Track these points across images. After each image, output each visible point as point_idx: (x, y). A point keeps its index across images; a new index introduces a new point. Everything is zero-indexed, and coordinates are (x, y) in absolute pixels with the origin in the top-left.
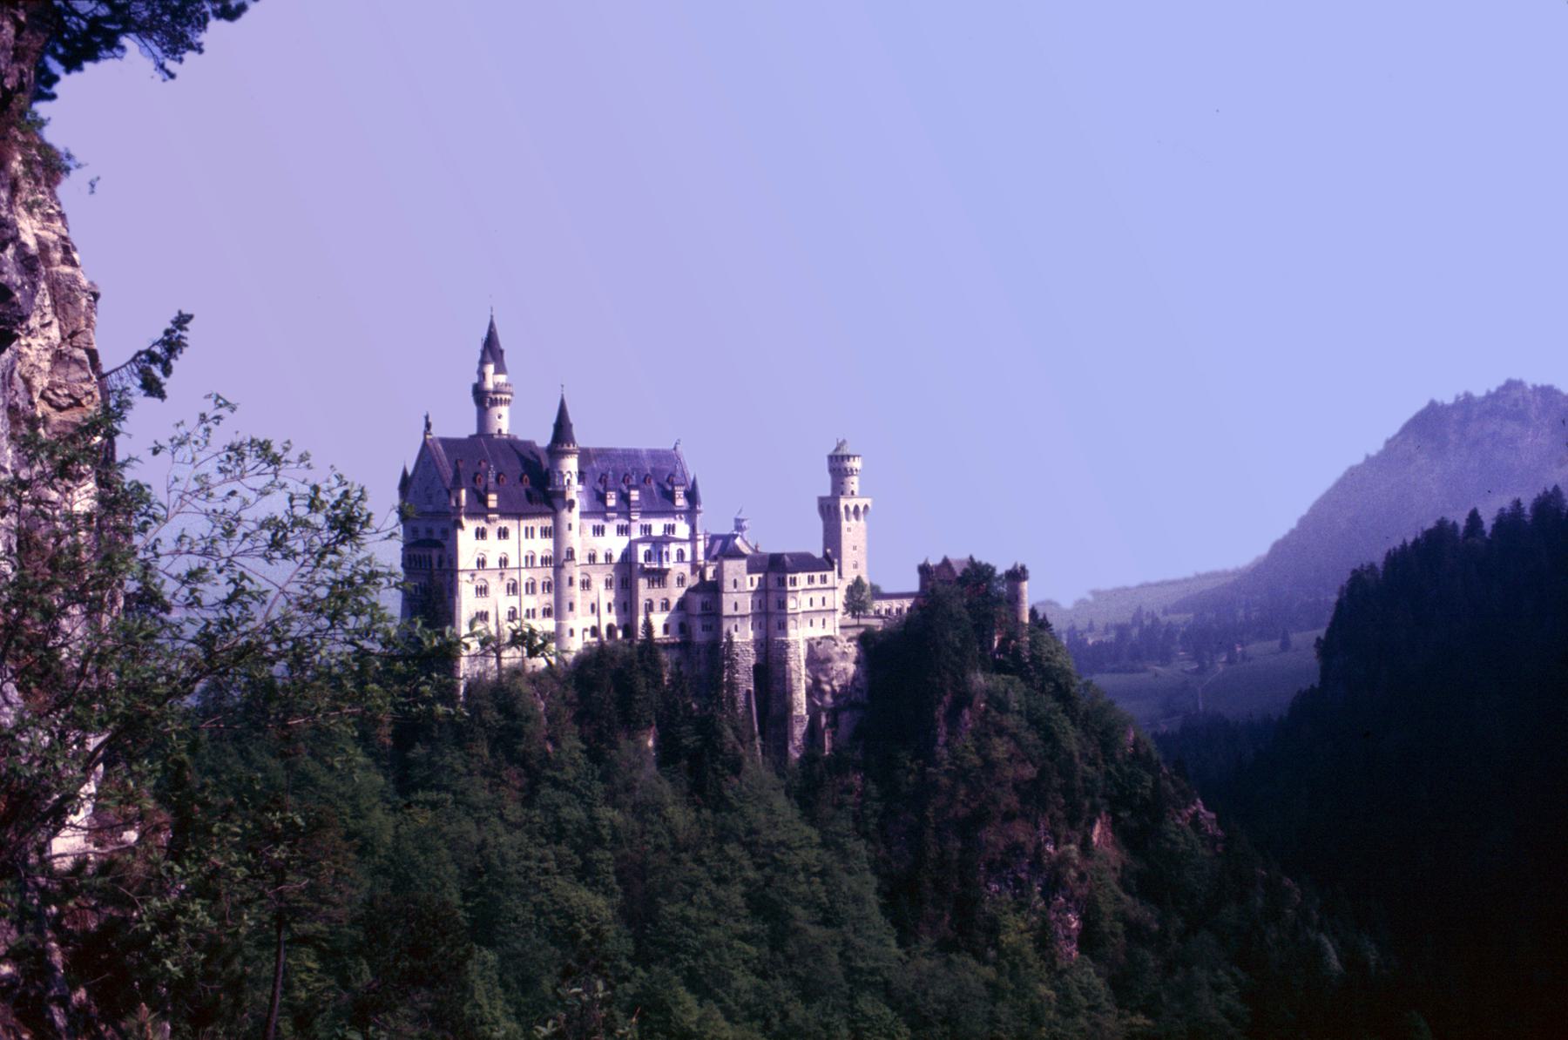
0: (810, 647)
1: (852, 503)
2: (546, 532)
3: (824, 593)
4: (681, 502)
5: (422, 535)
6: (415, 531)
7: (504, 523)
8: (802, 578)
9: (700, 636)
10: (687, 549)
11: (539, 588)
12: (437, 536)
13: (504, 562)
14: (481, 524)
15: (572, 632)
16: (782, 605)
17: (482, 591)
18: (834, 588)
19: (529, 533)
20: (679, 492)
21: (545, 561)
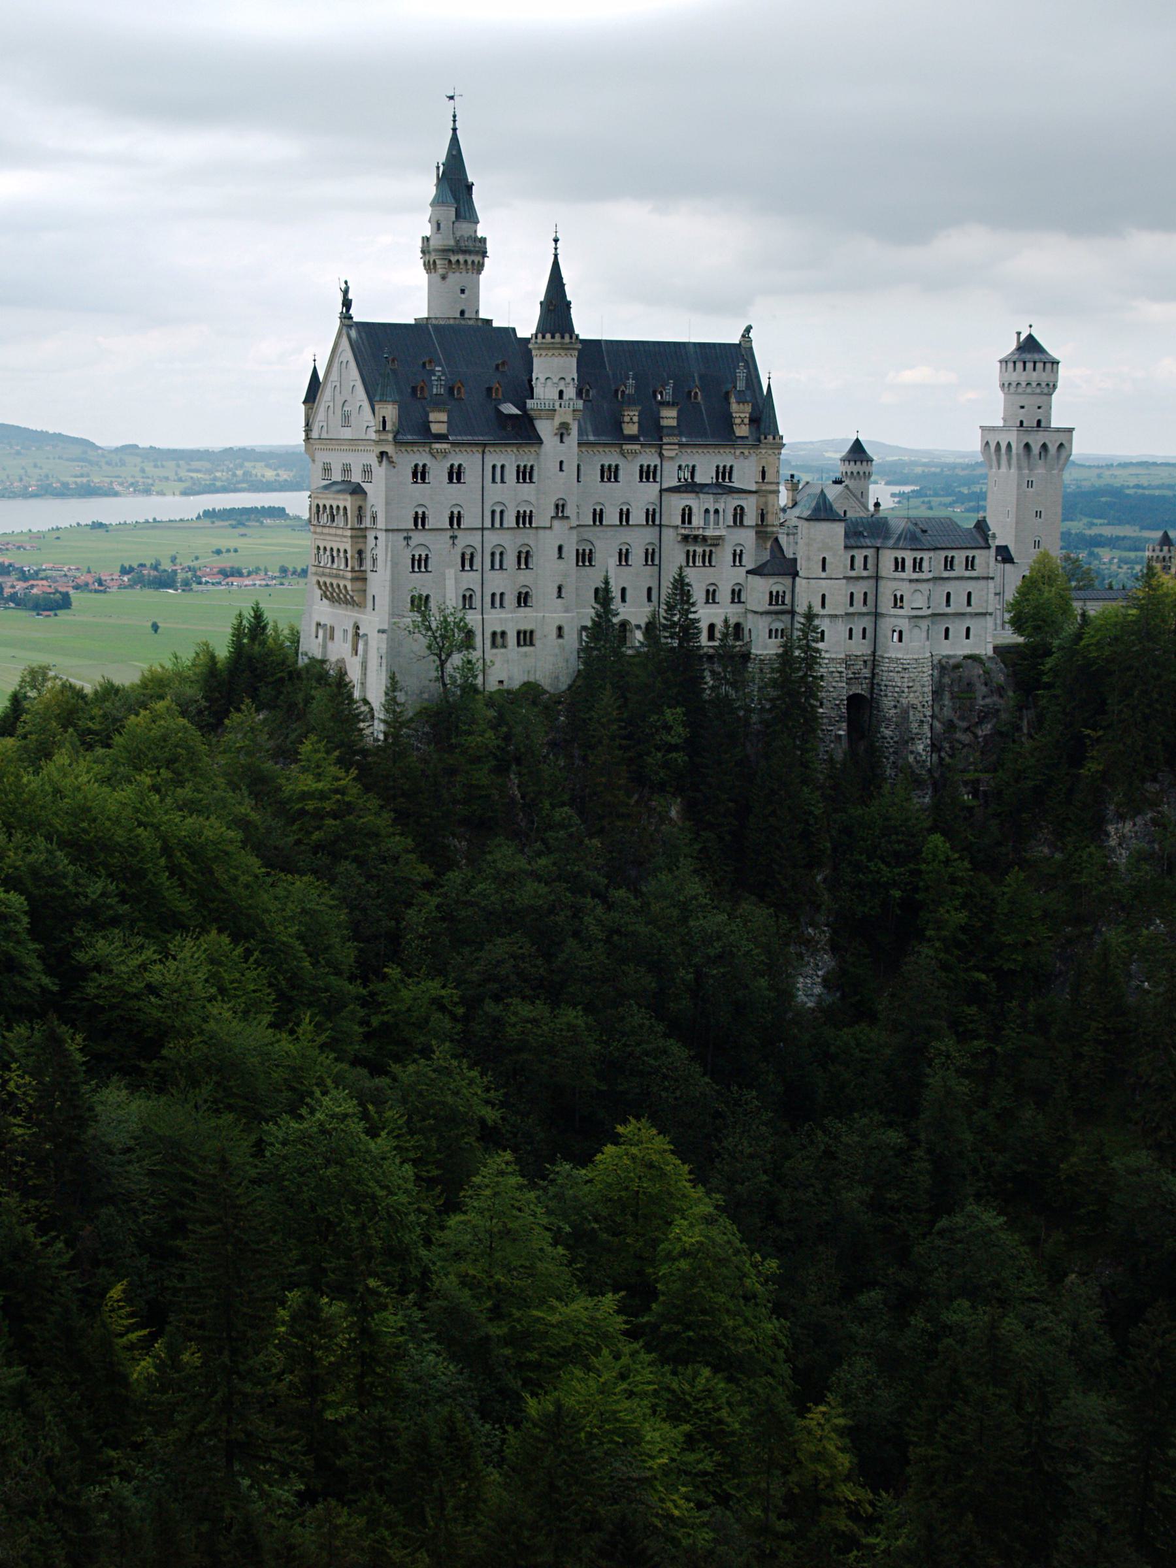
2: (525, 475)
3: (970, 586)
4: (742, 431)
5: (337, 476)
6: (327, 469)
8: (933, 562)
10: (750, 505)
11: (510, 560)
12: (356, 477)
13: (455, 519)
14: (421, 457)
15: (560, 628)
16: (898, 601)
18: (988, 578)
20: (740, 412)
21: (524, 519)
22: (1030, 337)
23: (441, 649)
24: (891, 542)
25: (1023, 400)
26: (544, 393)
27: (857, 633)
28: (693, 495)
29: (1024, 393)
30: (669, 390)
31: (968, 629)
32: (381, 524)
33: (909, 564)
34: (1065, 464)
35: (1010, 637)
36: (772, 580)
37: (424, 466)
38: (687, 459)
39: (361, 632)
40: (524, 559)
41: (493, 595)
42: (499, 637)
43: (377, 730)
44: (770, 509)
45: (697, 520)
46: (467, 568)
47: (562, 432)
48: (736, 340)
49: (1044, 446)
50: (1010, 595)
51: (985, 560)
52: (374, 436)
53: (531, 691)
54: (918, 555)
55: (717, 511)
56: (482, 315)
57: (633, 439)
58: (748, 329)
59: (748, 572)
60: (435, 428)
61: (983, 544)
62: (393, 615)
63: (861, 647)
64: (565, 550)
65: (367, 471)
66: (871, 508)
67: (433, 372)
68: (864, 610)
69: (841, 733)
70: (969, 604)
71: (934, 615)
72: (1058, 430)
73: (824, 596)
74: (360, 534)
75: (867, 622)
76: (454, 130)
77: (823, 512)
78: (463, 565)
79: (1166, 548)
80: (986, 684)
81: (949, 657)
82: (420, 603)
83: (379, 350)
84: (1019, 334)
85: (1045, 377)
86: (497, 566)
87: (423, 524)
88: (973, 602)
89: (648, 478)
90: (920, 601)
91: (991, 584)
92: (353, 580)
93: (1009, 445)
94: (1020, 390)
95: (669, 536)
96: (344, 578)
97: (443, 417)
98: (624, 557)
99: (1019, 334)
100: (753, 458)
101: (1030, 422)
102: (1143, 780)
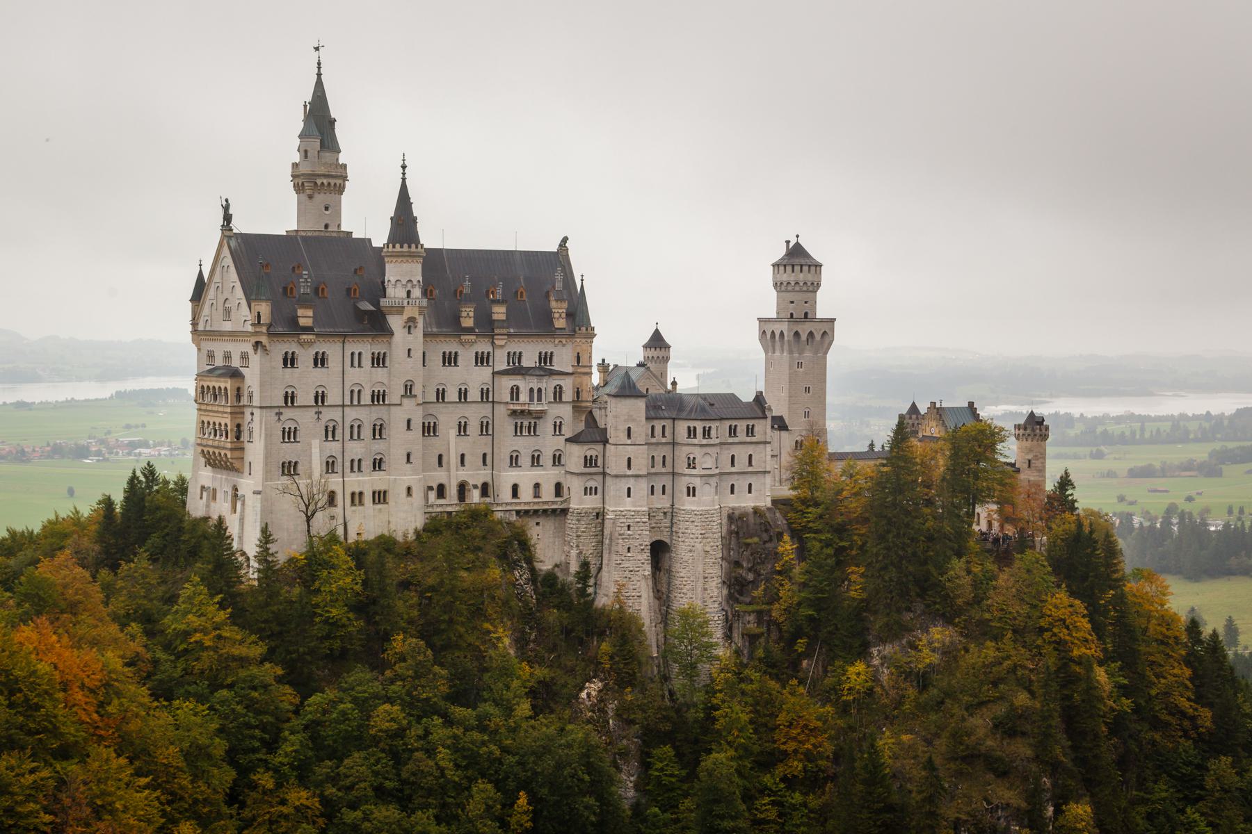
0: (731, 518)
1: (804, 329)
2: (379, 360)
3: (750, 450)
4: (560, 323)
5: (219, 362)
6: (211, 356)
7: (322, 347)
8: (720, 430)
9: (579, 501)
10: (568, 384)
11: (367, 432)
12: (236, 363)
13: (320, 398)
14: (291, 347)
15: (409, 489)
16: (691, 464)
17: (290, 435)
18: (766, 443)
19: (356, 360)
20: (559, 310)
21: (379, 398)
22: (798, 245)
23: (307, 507)
24: (684, 415)
25: (790, 296)
26: (395, 293)
27: (658, 489)
28: (519, 377)
29: (793, 291)
30: (499, 290)
31: (750, 485)
32: (256, 402)
33: (699, 431)
34: (828, 348)
35: (786, 492)
36: (586, 447)
37: (293, 353)
38: (515, 347)
39: (239, 493)
40: (378, 431)
41: (352, 461)
42: (357, 497)
43: (252, 574)
44: (584, 387)
45: (524, 397)
46: (330, 438)
47: (410, 324)
48: (554, 248)
49: (811, 334)
50: (786, 459)
51: (763, 428)
52: (250, 329)
53: (385, 544)
54: (707, 424)
55: (540, 390)
56: (343, 228)
57: (469, 330)
58: (565, 240)
59: (567, 440)
60: (302, 322)
61: (760, 415)
62: (266, 479)
63: (662, 502)
64: (412, 423)
65: (244, 357)
66: (669, 387)
67: (301, 276)
68: (664, 470)
69: (647, 573)
70: (750, 464)
71: (721, 474)
72: (822, 321)
73: (629, 459)
74: (238, 412)
75: (667, 481)
76: (319, 75)
77: (628, 390)
78: (327, 436)
79: (914, 416)
80: (766, 531)
81: (733, 509)
82: (289, 469)
83: (254, 258)
84: (788, 242)
85: (810, 278)
86: (355, 437)
87: (292, 402)
88: (753, 463)
89: (482, 363)
90: (709, 463)
91: (768, 447)
92: (231, 449)
93: (782, 333)
94: (790, 288)
95: (501, 411)
96: (224, 448)
97: (310, 313)
98: (462, 429)
99: (788, 242)
100: (569, 346)
101: (799, 314)
102: (899, 611)
